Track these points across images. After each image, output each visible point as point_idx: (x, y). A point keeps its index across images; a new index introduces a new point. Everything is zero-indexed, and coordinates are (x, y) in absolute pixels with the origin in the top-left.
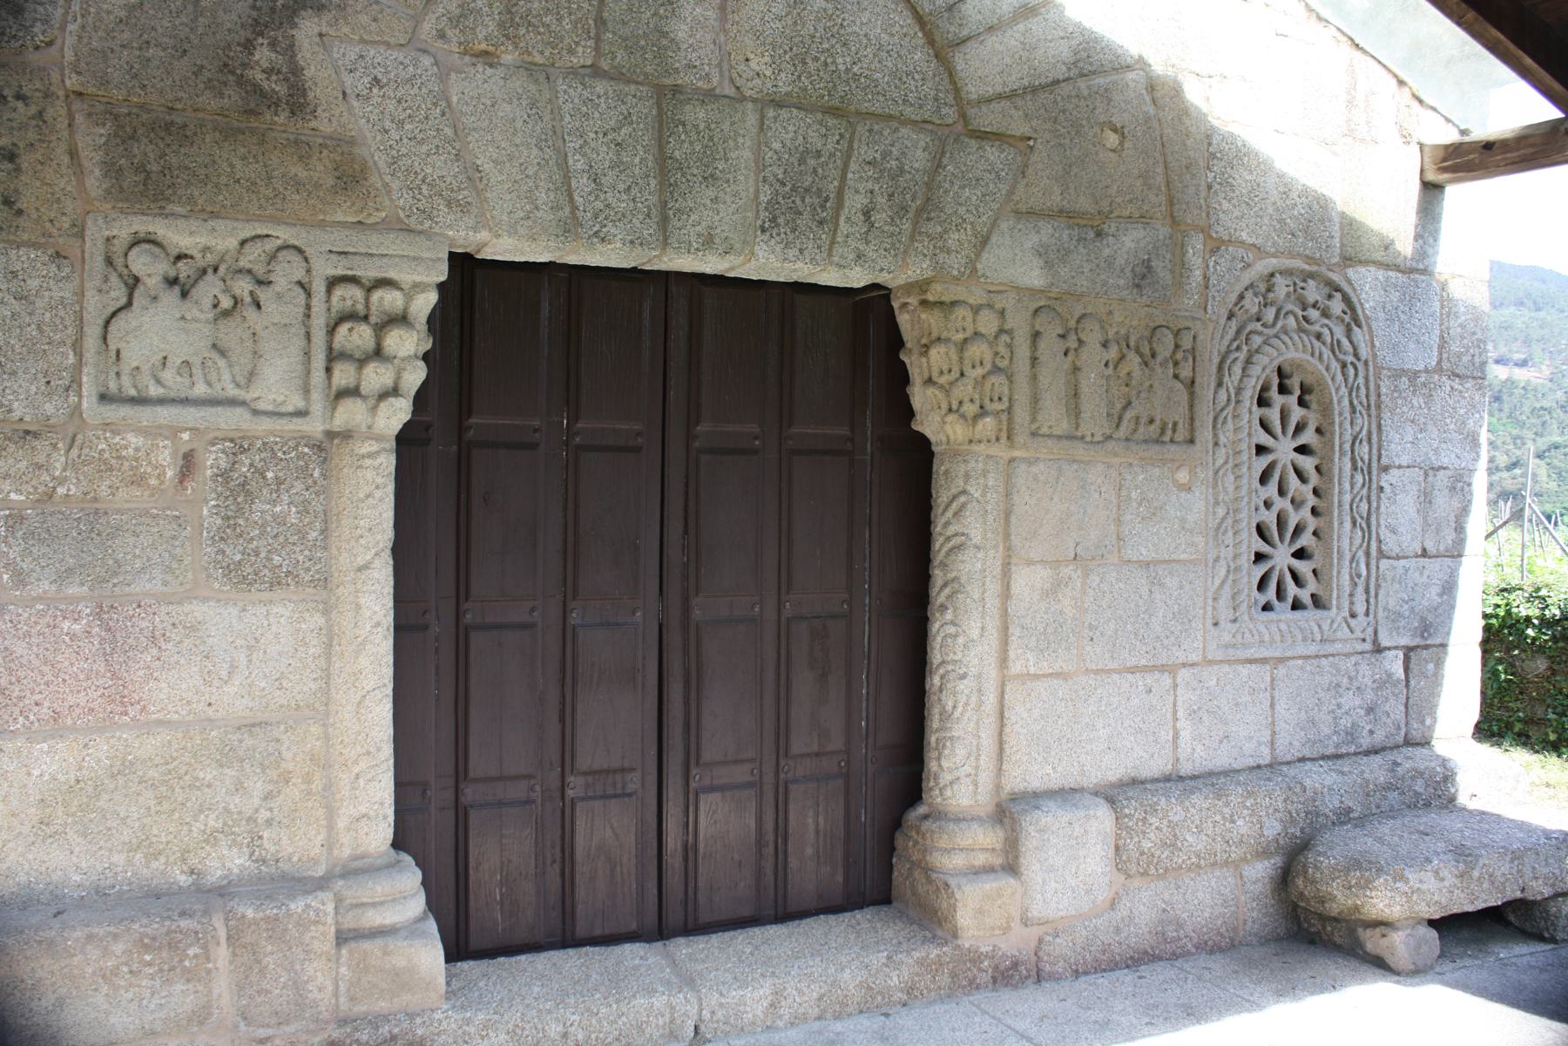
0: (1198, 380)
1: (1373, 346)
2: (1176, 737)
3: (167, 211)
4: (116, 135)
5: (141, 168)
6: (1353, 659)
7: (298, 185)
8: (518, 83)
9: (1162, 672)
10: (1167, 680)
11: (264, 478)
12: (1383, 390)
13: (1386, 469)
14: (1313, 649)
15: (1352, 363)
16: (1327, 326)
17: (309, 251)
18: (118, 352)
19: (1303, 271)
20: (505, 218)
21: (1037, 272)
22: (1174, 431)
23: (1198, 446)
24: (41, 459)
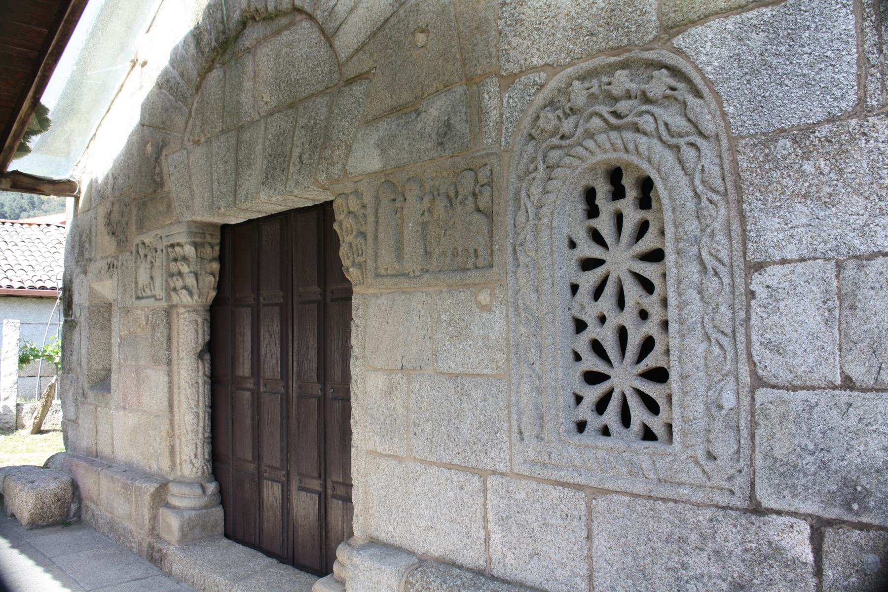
0: (495, 208)
1: (724, 114)
2: (487, 540)
6: (708, 513)
9: (474, 474)
10: (476, 483)
14: (640, 487)
15: (692, 144)
16: (648, 112)
19: (610, 65)
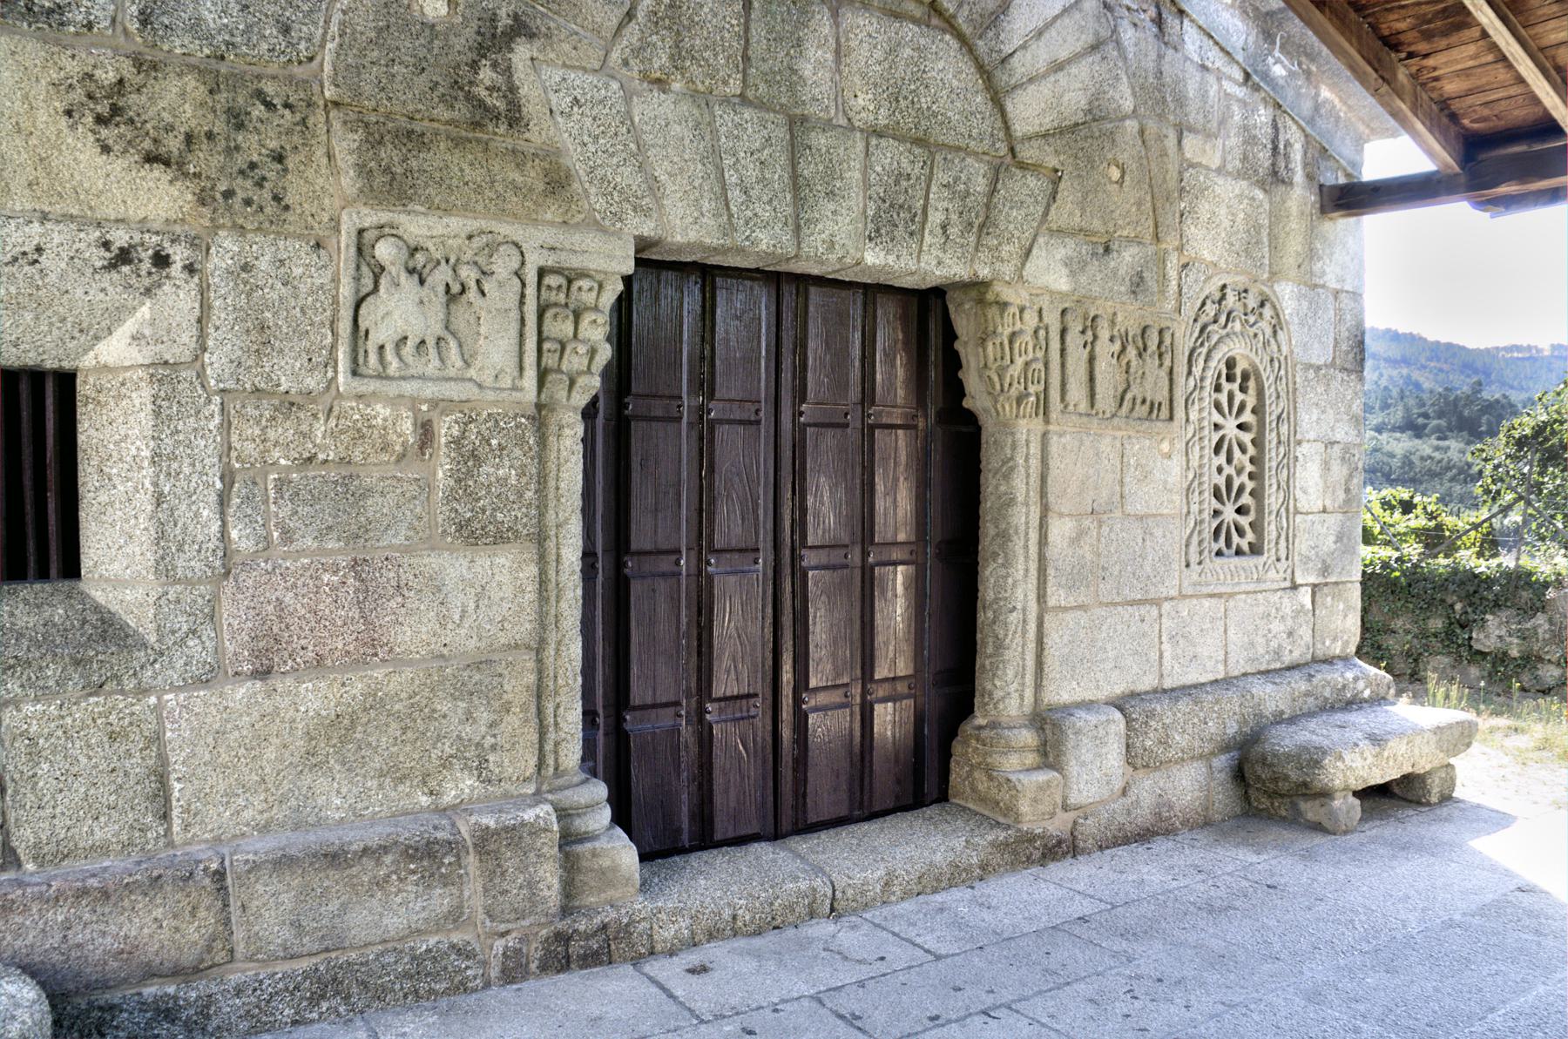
2: (1161, 657)
3: (409, 208)
4: (367, 141)
5: (387, 170)
6: (1279, 593)
7: (516, 189)
8: (685, 107)
9: (1151, 604)
10: (1155, 612)
11: (490, 445)
12: (1298, 380)
13: (1299, 443)
14: (1251, 587)
17: (525, 247)
18: (367, 332)
20: (678, 222)
21: (1064, 280)
22: (1159, 410)
23: (1176, 423)
24: (304, 428)
